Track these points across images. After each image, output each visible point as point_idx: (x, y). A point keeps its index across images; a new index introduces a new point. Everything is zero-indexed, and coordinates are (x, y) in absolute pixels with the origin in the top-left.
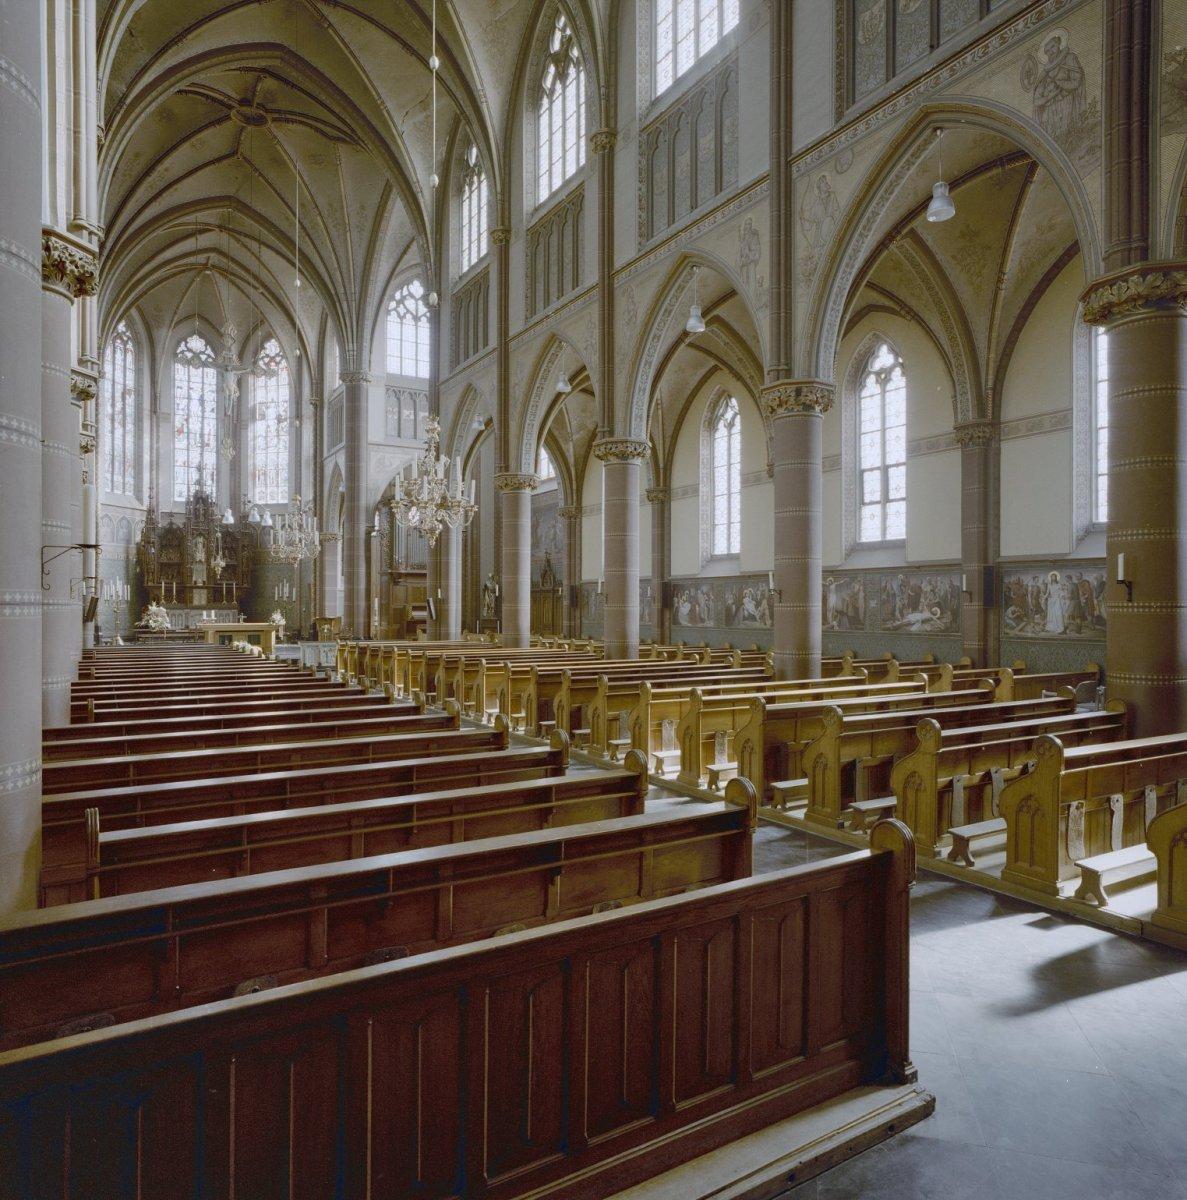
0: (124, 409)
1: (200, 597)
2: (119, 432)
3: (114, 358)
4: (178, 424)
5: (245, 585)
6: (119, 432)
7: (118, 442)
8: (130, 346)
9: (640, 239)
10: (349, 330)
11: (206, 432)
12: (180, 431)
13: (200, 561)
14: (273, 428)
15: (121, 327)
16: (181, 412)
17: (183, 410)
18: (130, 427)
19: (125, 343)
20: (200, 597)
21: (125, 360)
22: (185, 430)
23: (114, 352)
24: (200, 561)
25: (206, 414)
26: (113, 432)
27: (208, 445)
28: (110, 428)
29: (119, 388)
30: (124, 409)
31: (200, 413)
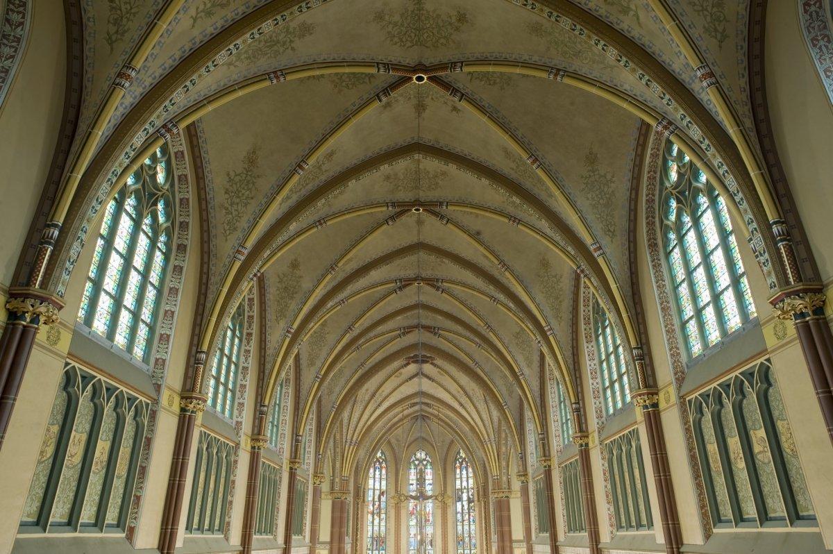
0: (379, 505)
2: (376, 522)
3: (375, 474)
4: (411, 509)
6: (376, 522)
7: (376, 528)
8: (384, 465)
9: (611, 529)
10: (492, 457)
12: (412, 514)
14: (466, 507)
15: (379, 455)
18: (383, 516)
19: (380, 464)
21: (381, 474)
23: (375, 471)
26: (373, 522)
27: (429, 520)
28: (371, 520)
29: (377, 493)
30: (379, 505)
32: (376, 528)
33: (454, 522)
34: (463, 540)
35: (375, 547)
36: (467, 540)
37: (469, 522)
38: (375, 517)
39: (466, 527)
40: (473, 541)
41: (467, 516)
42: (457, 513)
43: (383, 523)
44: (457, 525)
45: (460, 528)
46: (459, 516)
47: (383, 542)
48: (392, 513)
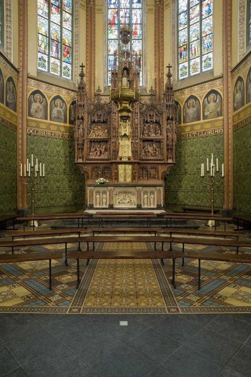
1: (125, 173)
4: (110, 17)
5: (170, 161)
6: (55, 17)
7: (55, 28)
11: (134, 21)
12: (112, 24)
13: (125, 135)
16: (112, 6)
17: (114, 3)
18: (67, 16)
20: (125, 173)
22: (116, 22)
24: (125, 135)
25: (134, 6)
31: (128, 5)
32: (55, 28)
33: (173, 27)
34: (188, 47)
35: (53, 54)
36: (195, 45)
37: (201, 15)
38: (53, 9)
39: (195, 28)
40: (207, 41)
41: (198, 8)
42: (178, 15)
43: (67, 25)
44: (178, 31)
45: (183, 36)
46: (183, 18)
47: (68, 53)
48: (82, 14)
